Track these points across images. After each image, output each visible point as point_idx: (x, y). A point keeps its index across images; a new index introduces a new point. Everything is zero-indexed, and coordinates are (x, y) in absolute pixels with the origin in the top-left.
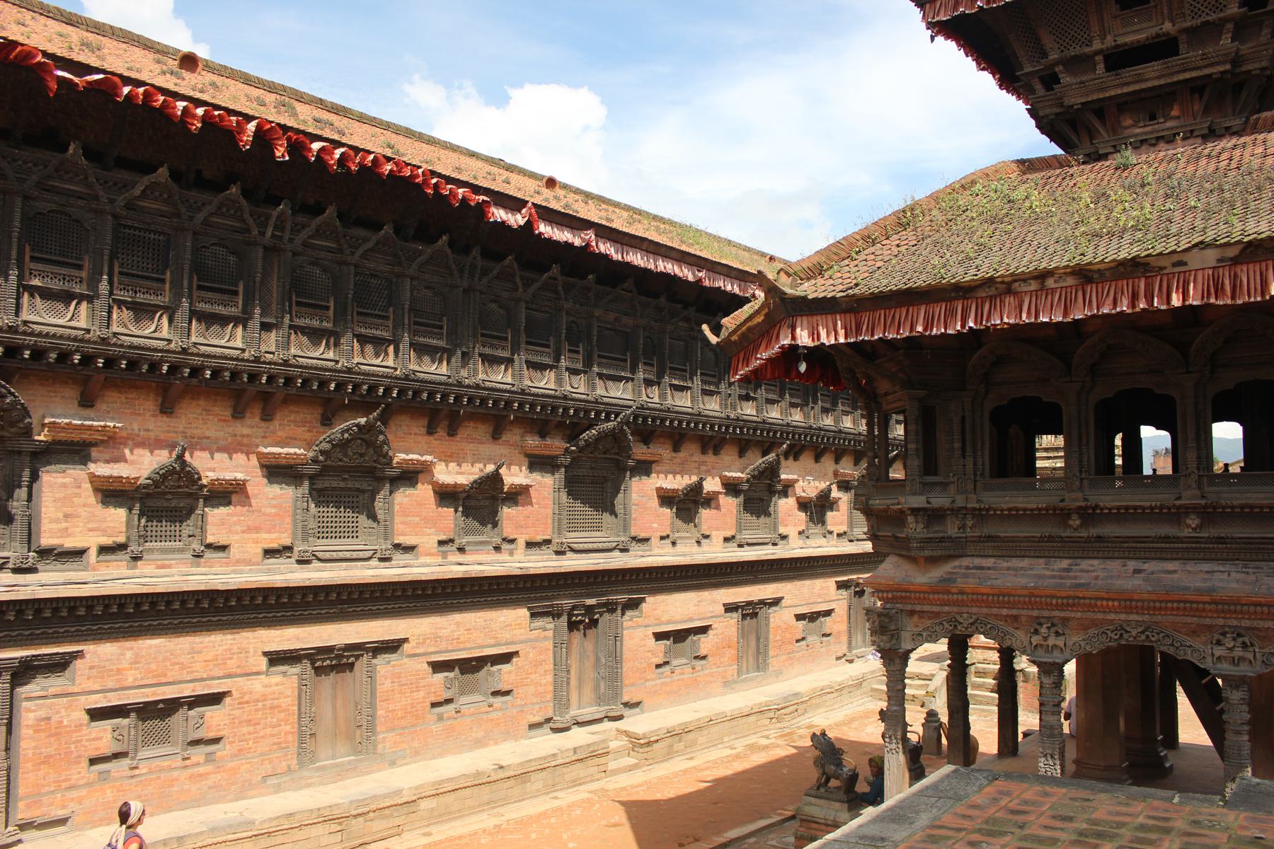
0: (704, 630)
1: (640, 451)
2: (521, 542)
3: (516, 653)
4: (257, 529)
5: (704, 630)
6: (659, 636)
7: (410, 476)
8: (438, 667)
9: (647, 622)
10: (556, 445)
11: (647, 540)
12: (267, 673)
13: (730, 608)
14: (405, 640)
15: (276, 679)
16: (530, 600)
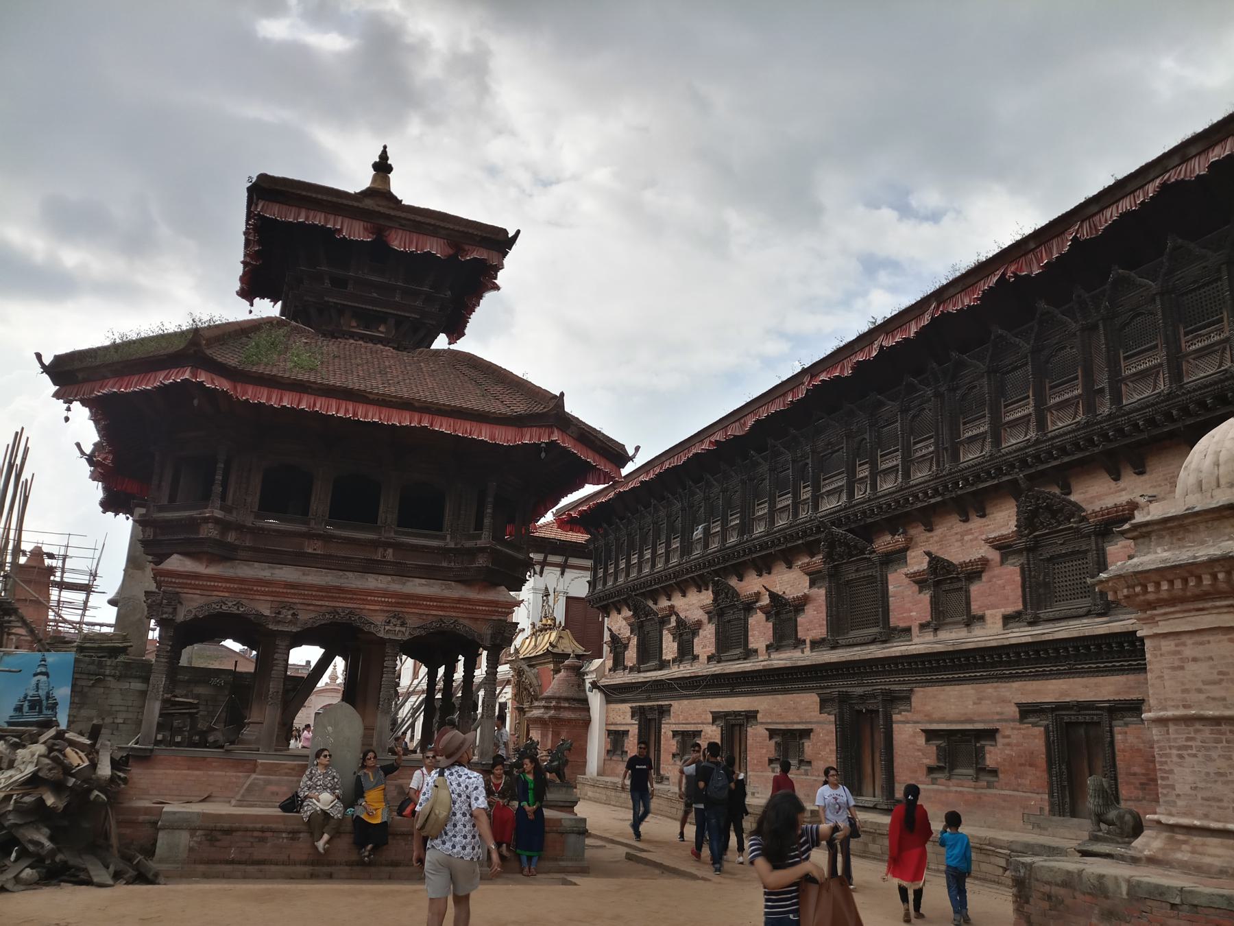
0: (991, 734)
1: (885, 542)
2: (808, 642)
3: (811, 730)
4: (704, 647)
5: (991, 734)
6: (930, 735)
7: (749, 607)
8: (772, 733)
9: (916, 717)
10: (818, 559)
11: (908, 630)
12: (713, 723)
13: (1027, 711)
14: (757, 712)
15: (714, 728)
16: (817, 688)
